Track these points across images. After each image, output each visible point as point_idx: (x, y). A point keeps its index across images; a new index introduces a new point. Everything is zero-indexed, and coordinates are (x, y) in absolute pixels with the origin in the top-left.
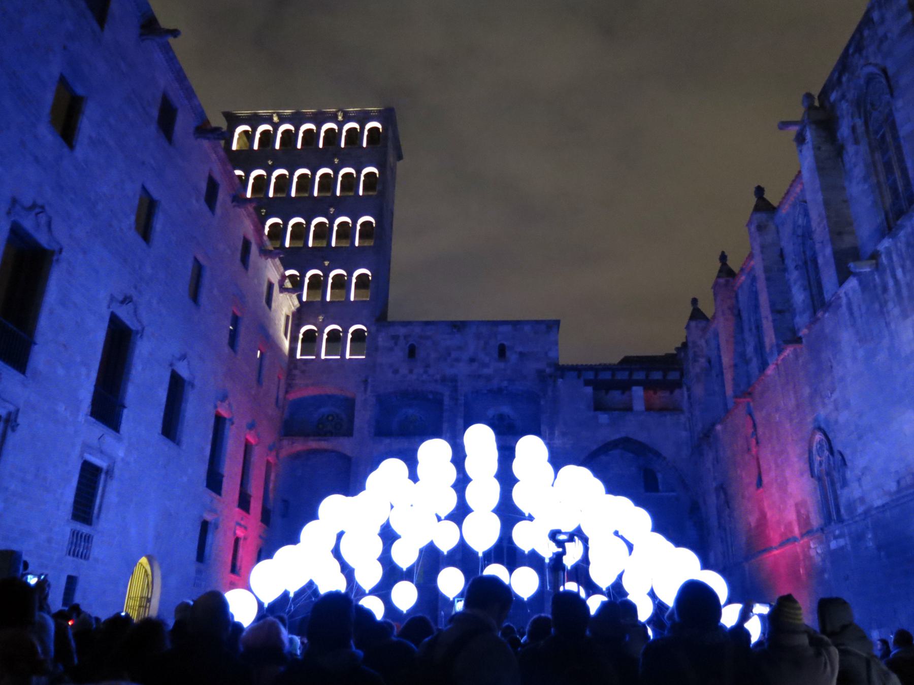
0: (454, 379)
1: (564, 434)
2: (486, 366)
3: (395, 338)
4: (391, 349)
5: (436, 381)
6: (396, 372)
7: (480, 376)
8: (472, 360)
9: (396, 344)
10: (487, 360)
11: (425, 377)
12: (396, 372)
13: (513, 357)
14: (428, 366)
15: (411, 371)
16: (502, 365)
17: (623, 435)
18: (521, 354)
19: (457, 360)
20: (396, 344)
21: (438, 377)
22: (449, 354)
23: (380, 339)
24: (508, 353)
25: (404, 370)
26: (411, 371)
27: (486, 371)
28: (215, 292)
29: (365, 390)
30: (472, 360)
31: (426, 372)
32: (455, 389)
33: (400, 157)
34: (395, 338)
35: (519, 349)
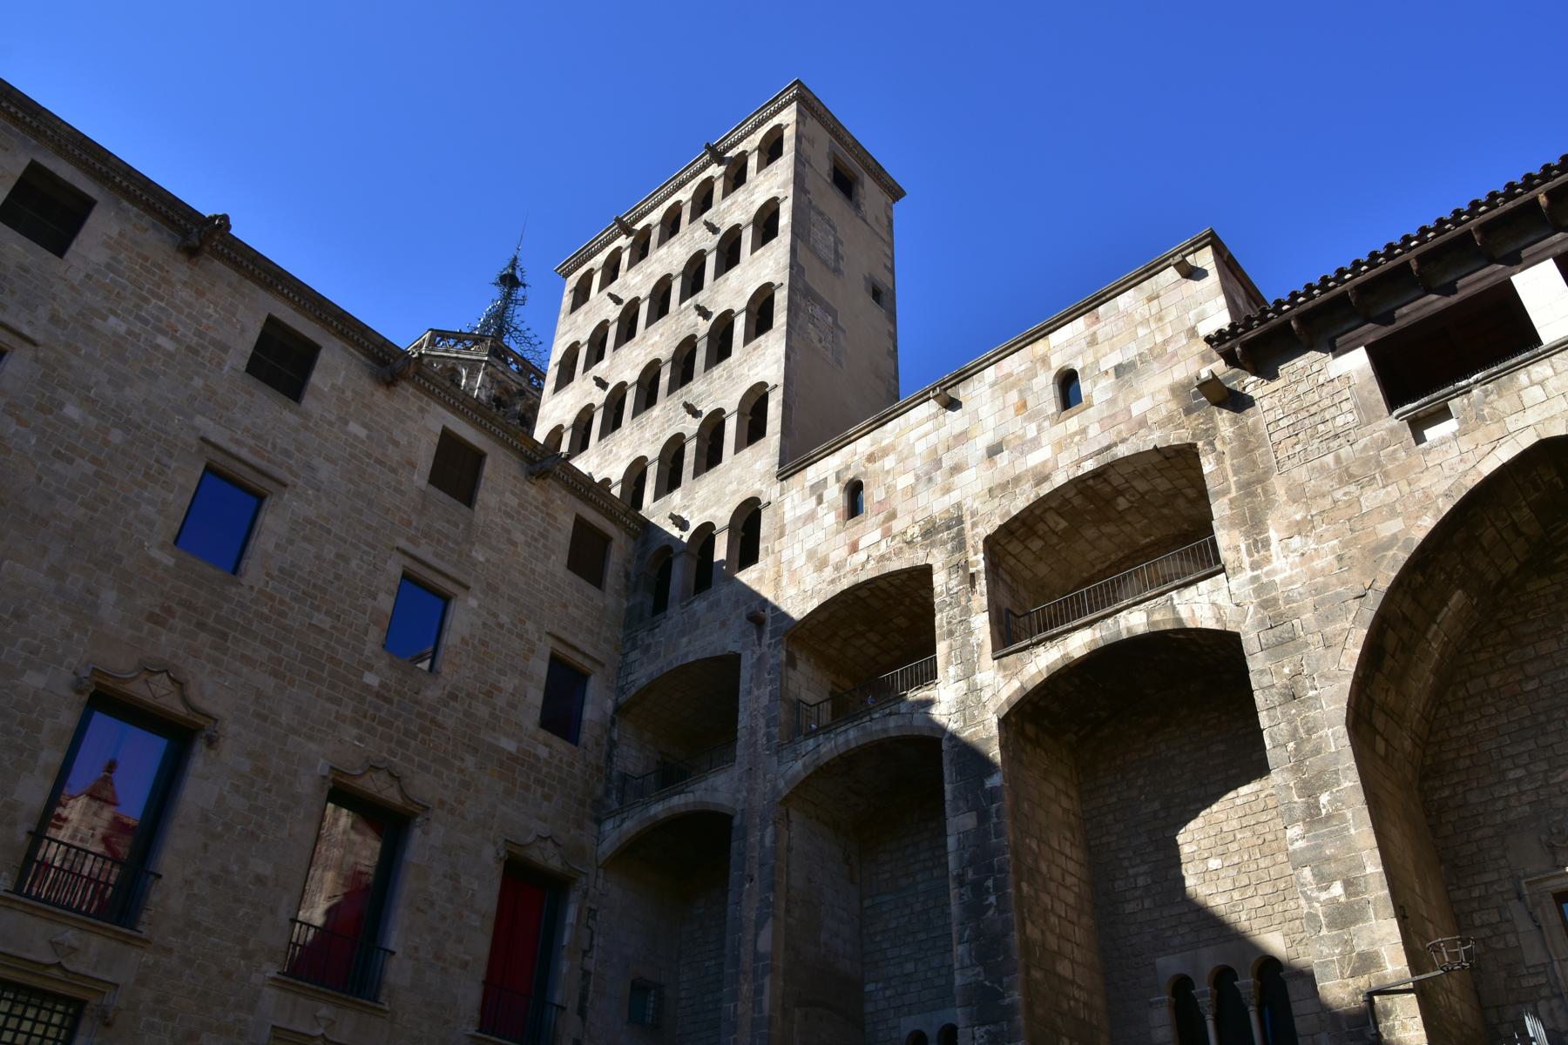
0: (955, 521)
2: (1035, 444)
6: (822, 565)
7: (1017, 480)
9: (820, 501)
10: (1032, 430)
13: (1093, 389)
14: (892, 516)
15: (854, 548)
16: (1073, 423)
17: (1527, 440)
18: (1120, 370)
19: (956, 469)
20: (820, 501)
21: (917, 530)
22: (938, 463)
23: (787, 506)
24: (1085, 387)
25: (838, 554)
27: (1034, 459)
28: (72, 411)
29: (760, 638)
30: (994, 451)
31: (887, 533)
32: (960, 545)
33: (896, 193)
34: (818, 490)
35: (1111, 361)
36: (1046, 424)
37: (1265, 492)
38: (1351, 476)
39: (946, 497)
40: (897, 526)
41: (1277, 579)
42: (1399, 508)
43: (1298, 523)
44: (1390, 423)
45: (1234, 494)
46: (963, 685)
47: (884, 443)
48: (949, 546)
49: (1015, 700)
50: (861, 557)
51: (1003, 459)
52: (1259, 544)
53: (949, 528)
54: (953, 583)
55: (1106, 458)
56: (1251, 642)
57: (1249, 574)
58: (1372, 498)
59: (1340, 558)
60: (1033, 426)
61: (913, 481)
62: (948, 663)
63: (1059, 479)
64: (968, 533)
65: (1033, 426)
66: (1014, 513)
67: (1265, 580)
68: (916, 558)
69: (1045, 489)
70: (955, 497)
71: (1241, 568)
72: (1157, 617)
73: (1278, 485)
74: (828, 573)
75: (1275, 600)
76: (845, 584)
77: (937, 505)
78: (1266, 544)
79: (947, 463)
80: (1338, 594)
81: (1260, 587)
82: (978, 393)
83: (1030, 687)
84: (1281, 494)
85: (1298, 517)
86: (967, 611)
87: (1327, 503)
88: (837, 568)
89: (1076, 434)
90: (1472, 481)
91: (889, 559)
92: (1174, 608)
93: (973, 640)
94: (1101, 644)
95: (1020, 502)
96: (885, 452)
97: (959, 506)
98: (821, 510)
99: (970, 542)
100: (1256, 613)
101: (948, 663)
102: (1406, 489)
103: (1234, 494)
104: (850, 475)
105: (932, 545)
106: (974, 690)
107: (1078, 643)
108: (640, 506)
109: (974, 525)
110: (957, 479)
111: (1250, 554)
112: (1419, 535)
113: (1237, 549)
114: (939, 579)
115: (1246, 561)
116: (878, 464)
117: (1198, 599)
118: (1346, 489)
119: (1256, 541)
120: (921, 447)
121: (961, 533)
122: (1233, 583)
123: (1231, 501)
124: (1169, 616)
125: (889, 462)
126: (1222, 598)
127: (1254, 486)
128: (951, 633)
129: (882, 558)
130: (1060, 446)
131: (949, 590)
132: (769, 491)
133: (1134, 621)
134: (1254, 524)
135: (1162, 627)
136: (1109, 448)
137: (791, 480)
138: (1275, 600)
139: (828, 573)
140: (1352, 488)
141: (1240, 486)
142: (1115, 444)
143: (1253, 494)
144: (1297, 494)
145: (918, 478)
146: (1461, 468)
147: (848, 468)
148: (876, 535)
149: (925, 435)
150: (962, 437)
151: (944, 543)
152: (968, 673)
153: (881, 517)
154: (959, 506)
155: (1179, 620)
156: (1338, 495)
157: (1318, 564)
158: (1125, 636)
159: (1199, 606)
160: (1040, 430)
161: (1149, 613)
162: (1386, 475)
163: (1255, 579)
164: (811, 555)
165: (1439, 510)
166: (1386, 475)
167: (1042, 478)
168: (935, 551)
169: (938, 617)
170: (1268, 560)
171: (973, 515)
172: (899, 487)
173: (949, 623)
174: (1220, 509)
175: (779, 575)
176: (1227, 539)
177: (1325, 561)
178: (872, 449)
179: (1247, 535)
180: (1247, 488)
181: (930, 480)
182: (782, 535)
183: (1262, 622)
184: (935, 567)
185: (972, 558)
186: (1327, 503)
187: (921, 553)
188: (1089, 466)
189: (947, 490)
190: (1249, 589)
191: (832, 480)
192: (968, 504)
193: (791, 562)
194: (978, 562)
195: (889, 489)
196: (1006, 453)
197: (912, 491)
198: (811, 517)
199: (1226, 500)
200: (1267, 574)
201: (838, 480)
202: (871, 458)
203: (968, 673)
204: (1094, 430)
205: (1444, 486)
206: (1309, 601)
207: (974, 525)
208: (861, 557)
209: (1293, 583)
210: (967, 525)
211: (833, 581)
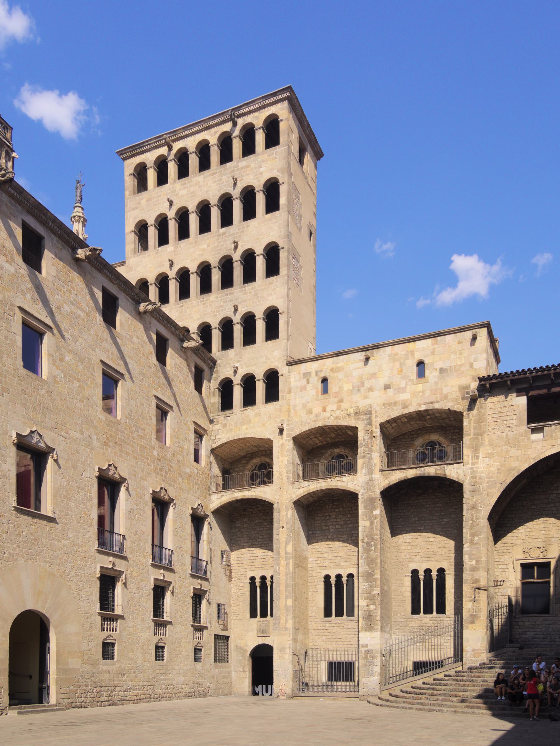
1: (490, 456)
2: (404, 390)
3: (307, 375)
4: (304, 388)
5: (349, 415)
6: (310, 412)
7: (395, 403)
8: (387, 387)
9: (308, 382)
10: (403, 385)
11: (338, 413)
12: (310, 412)
14: (341, 401)
15: (324, 410)
19: (370, 389)
20: (308, 382)
21: (351, 411)
22: (363, 384)
23: (292, 380)
25: (317, 410)
26: (324, 410)
30: (387, 387)
31: (339, 408)
32: (370, 423)
34: (307, 375)
36: (409, 383)
37: (482, 439)
38: (509, 443)
39: (365, 401)
40: (344, 406)
41: (478, 470)
42: (520, 458)
43: (489, 453)
44: (524, 428)
45: (472, 436)
46: (368, 477)
47: (339, 365)
48: (365, 422)
49: (386, 487)
50: (327, 414)
51: (390, 392)
52: (476, 457)
53: (366, 414)
54: (366, 438)
55: (430, 407)
56: (467, 488)
57: (470, 466)
58: (513, 452)
59: (499, 469)
60: (404, 382)
61: (351, 388)
62: (362, 468)
63: (412, 409)
64: (374, 419)
65: (404, 382)
66: (393, 417)
67: (475, 470)
68: (352, 423)
69: (406, 411)
70: (368, 402)
71: (468, 464)
72: (438, 472)
73: (486, 437)
74: (312, 416)
75: (476, 477)
76: (320, 424)
77: (363, 404)
78: (478, 457)
79: (367, 385)
80: (495, 480)
81: (473, 471)
82: (381, 357)
83: (392, 484)
84: (486, 442)
85: (490, 451)
86: (371, 450)
87: (499, 450)
88: (317, 416)
89: (420, 392)
90: (542, 456)
91: (340, 419)
92: (444, 470)
93: (372, 461)
94: (418, 475)
95: (396, 413)
96: (339, 370)
97: (371, 406)
98: (309, 387)
99: (374, 423)
100: (470, 479)
101: (362, 468)
102: (523, 453)
103: (472, 436)
104: (323, 375)
105: (359, 419)
106: (371, 480)
107: (411, 473)
108: (210, 350)
109: (376, 417)
110: (370, 394)
111: (472, 459)
112: (523, 469)
113: (468, 456)
114: (361, 435)
115: (470, 461)
116: (335, 374)
117: (452, 470)
118: (506, 447)
119: (475, 456)
120: (355, 373)
121: (370, 418)
122: (465, 467)
123: (470, 439)
124: (443, 473)
125: (341, 375)
126: (460, 472)
127: (479, 435)
128: (364, 457)
129: (337, 418)
130: (414, 394)
131: (364, 440)
132: (283, 370)
133: (430, 470)
134: (476, 450)
135: (439, 475)
136: (432, 403)
137: (293, 367)
138: (476, 477)
139: (312, 416)
140: (509, 447)
141: (474, 435)
142: (435, 402)
143: (477, 438)
144: (491, 444)
145: (353, 387)
146: (541, 451)
147: (321, 371)
148: (334, 407)
149: (358, 368)
150: (373, 376)
151: (363, 420)
152: (370, 473)
153: (337, 399)
154: (371, 406)
155: (445, 475)
156: (504, 448)
157: (492, 469)
158: (426, 475)
159: (452, 472)
160: (406, 384)
161: (436, 470)
162: (519, 446)
163: (472, 468)
164: (304, 406)
165: (530, 463)
166: (519, 446)
167: (405, 407)
168: (359, 422)
169: (359, 449)
170: (477, 463)
171: (376, 412)
172: (345, 389)
173: (364, 453)
174: (466, 440)
175: (289, 410)
176: (467, 452)
177: (494, 469)
178: (333, 366)
179: (473, 452)
180: (476, 435)
181: (359, 390)
182: (290, 392)
183: (471, 483)
184: (359, 429)
185: (374, 430)
186: (499, 450)
187: (353, 421)
188: (424, 408)
189: (366, 397)
190: (469, 471)
191: (313, 374)
192: (375, 407)
193: (295, 406)
194: (377, 432)
195: (341, 388)
196: (391, 390)
197: (351, 392)
198: (304, 388)
199: (469, 438)
200: (476, 468)
201: (317, 375)
202: (332, 370)
203: (370, 473)
204: (428, 393)
205: (533, 456)
206: (486, 480)
207: (376, 417)
208: (327, 414)
209: (483, 473)
210: (373, 415)
211: (315, 421)
